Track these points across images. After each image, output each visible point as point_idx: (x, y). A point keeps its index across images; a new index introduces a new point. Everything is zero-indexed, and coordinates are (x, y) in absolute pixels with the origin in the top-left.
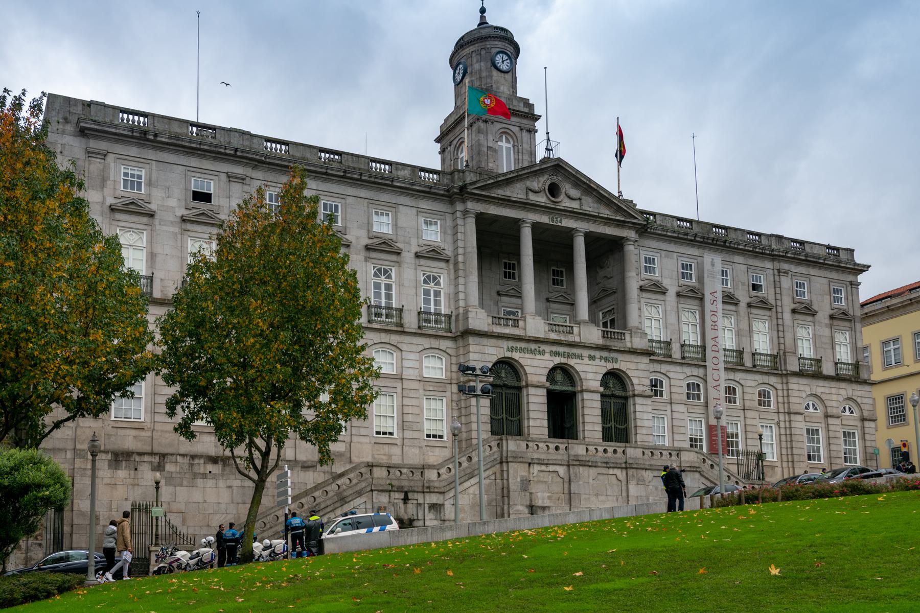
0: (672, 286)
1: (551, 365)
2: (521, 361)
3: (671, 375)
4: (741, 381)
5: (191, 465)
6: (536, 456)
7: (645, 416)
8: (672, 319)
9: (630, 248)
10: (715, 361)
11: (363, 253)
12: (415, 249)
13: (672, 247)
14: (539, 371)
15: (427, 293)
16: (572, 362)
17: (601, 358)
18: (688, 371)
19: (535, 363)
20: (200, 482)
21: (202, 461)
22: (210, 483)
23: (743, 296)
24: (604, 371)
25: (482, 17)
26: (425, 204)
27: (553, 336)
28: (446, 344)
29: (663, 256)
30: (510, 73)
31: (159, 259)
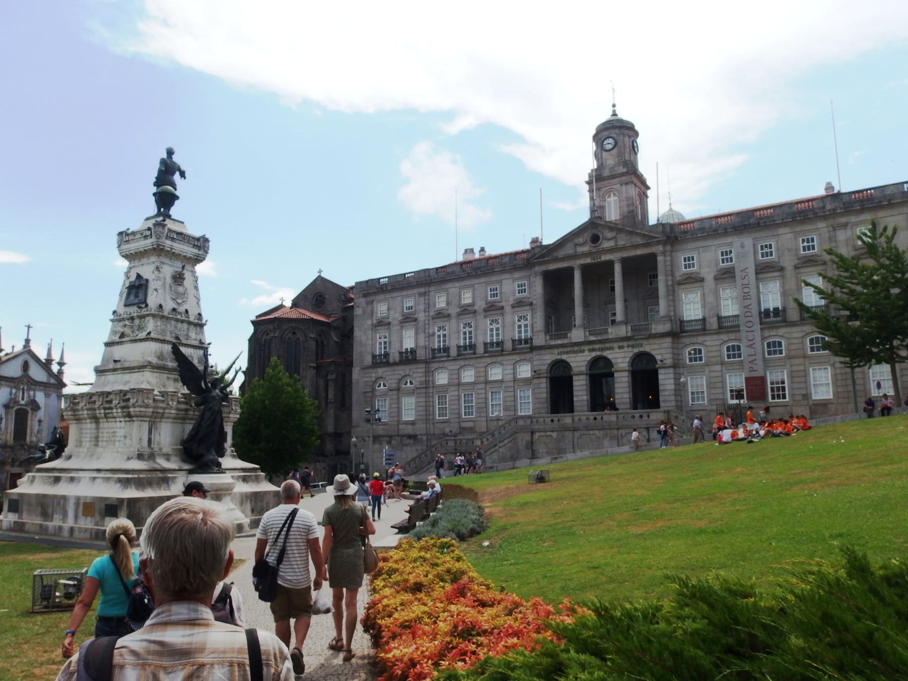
0: (708, 274)
1: (589, 358)
2: (569, 360)
3: (708, 343)
4: (785, 335)
5: (401, 440)
6: (537, 427)
7: (667, 382)
8: (710, 298)
9: (660, 259)
10: (749, 324)
11: (483, 314)
12: (511, 302)
13: (709, 242)
14: (581, 364)
15: (520, 327)
16: (605, 354)
17: (628, 346)
18: (725, 337)
19: (578, 359)
20: (405, 448)
21: (405, 438)
22: (409, 448)
23: (788, 262)
24: (631, 354)
25: (614, 111)
26: (516, 275)
27: (592, 338)
28: (528, 356)
29: (701, 251)
30: (616, 149)
31: (392, 343)
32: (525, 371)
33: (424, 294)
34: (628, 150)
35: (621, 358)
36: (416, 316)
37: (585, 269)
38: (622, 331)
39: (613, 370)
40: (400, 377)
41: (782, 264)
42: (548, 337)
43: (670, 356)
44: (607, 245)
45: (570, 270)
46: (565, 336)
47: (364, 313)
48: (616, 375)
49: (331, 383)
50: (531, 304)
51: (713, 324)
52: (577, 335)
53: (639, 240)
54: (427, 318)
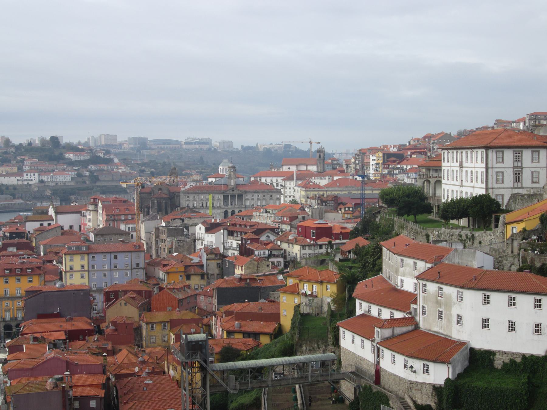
16: (235, 210)
23: (261, 198)
32: (219, 211)
33: (198, 195)
37: (231, 195)
38: (237, 206)
44: (235, 192)
45: (228, 195)
51: (250, 206)
52: (230, 206)
53: (240, 192)
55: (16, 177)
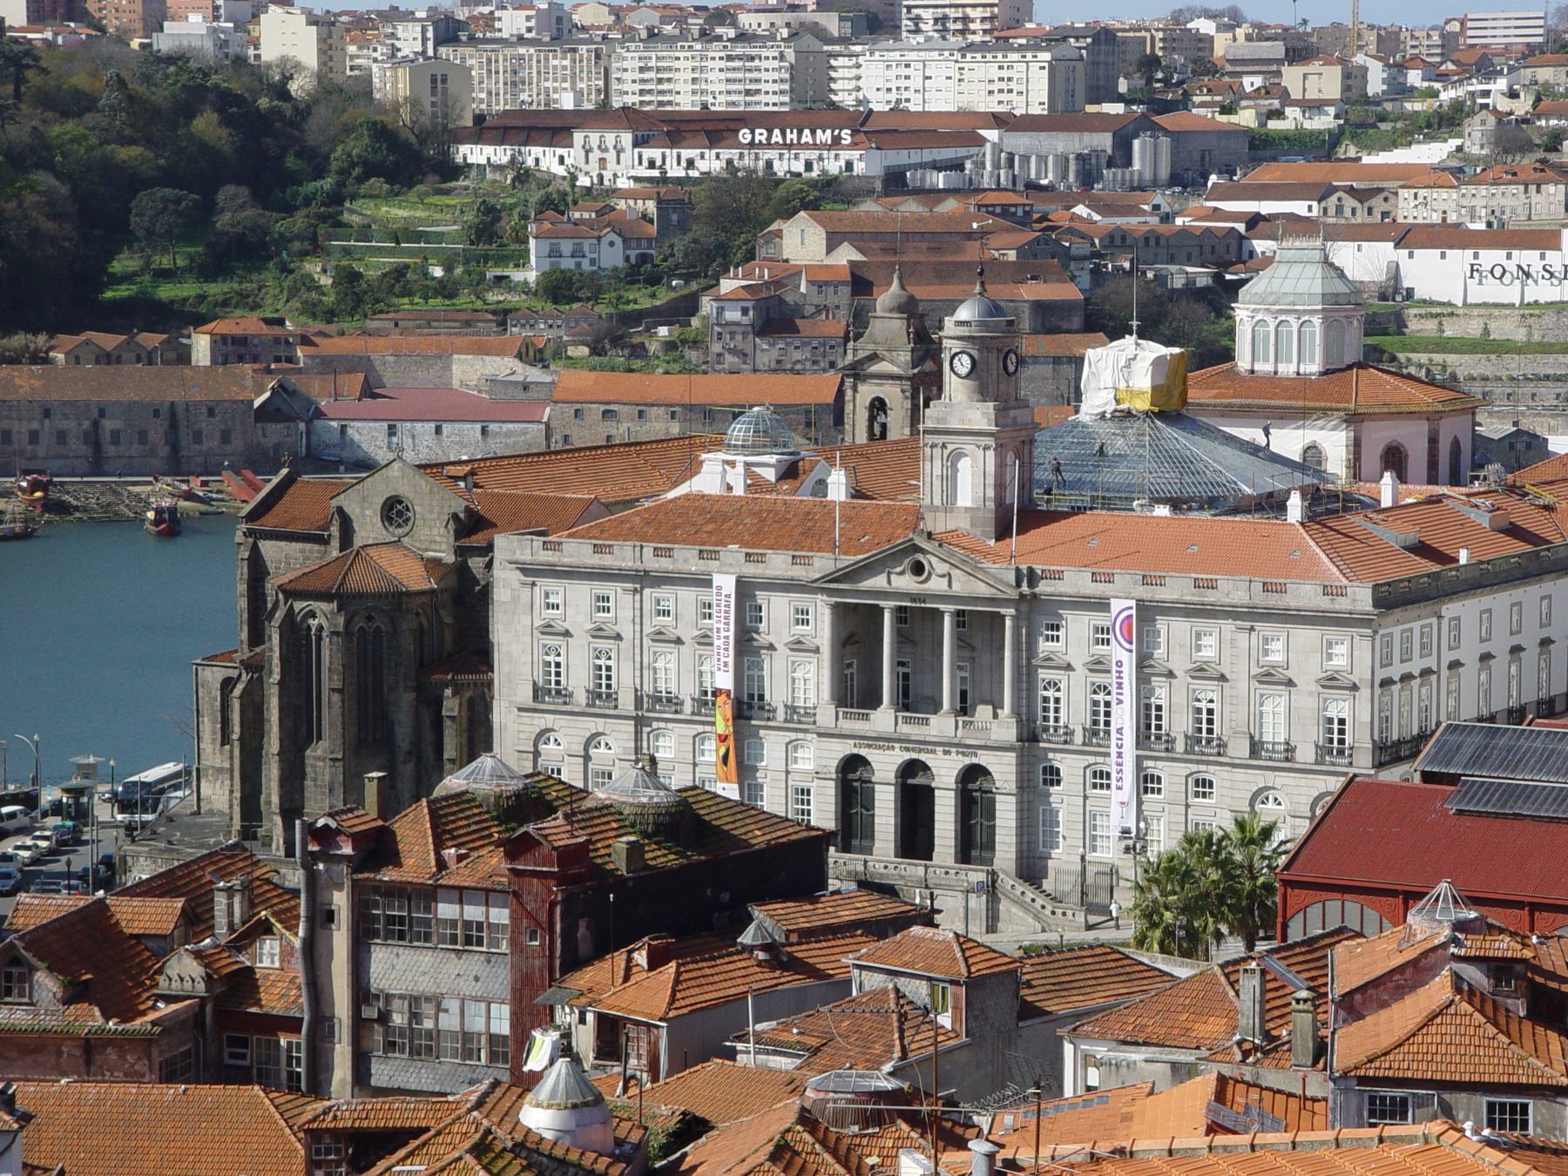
1: (900, 761)
2: (869, 758)
9: (1008, 623)
16: (923, 757)
17: (958, 753)
19: (882, 758)
23: (1180, 665)
24: (960, 766)
27: (905, 729)
34: (995, 376)
35: (945, 772)
36: (617, 628)
37: (901, 614)
39: (933, 785)
40: (588, 735)
41: (1170, 666)
42: (841, 714)
43: (1013, 777)
46: (866, 717)
47: (515, 600)
48: (937, 793)
49: (448, 723)
50: (818, 648)
52: (883, 718)
54: (638, 635)
55: (1515, 253)
